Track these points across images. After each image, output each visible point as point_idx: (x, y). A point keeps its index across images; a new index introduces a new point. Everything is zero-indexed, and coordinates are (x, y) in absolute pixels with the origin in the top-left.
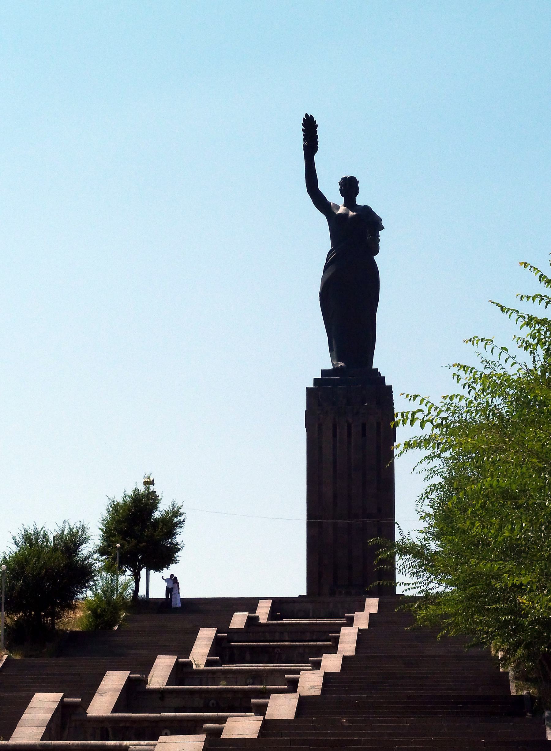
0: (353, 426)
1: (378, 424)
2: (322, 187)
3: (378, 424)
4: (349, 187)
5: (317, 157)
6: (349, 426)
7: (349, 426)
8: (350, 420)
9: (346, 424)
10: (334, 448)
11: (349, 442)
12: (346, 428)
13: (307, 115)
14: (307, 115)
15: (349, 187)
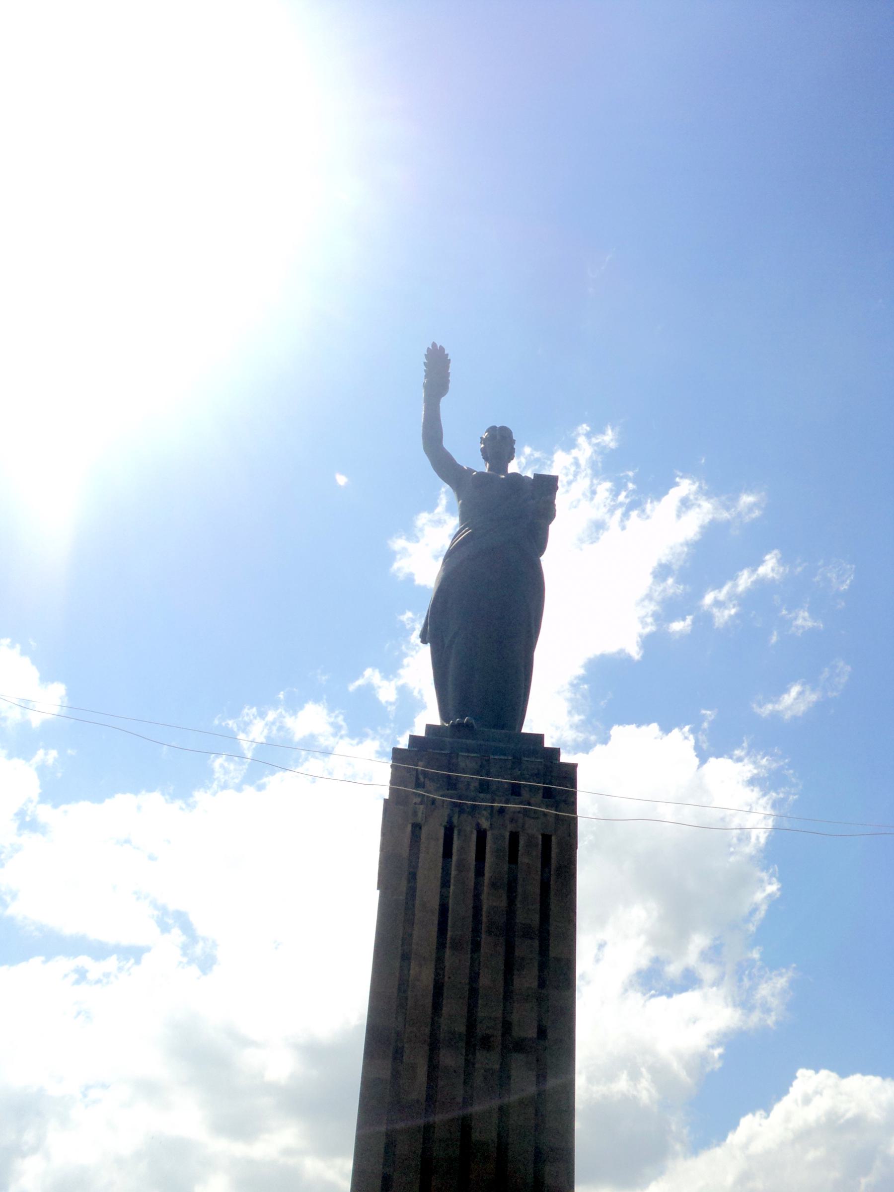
0: (489, 834)
1: (547, 839)
2: (448, 444)
3: (547, 839)
4: (499, 444)
5: (446, 404)
6: (482, 836)
7: (482, 836)
8: (485, 824)
9: (475, 832)
10: (445, 883)
11: (479, 872)
12: (474, 837)
13: (434, 344)
14: (434, 344)
15: (499, 444)
